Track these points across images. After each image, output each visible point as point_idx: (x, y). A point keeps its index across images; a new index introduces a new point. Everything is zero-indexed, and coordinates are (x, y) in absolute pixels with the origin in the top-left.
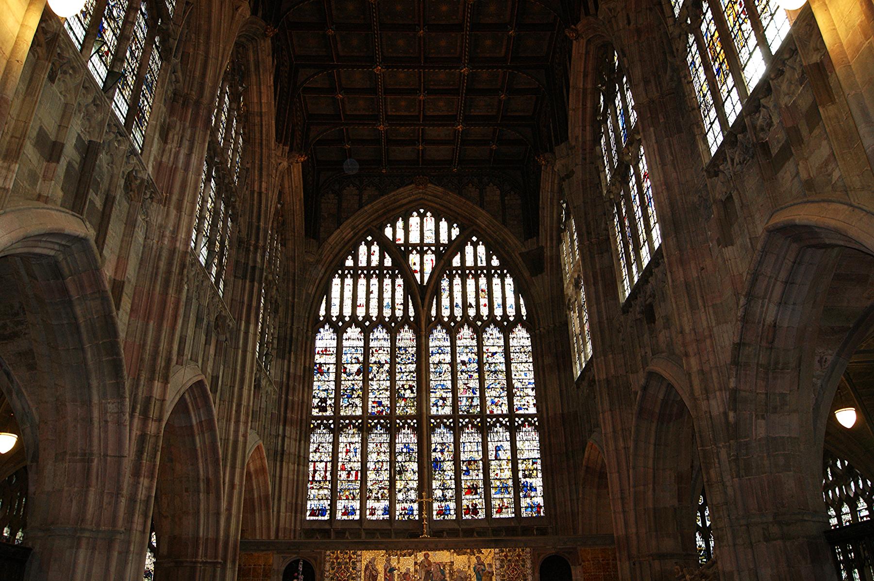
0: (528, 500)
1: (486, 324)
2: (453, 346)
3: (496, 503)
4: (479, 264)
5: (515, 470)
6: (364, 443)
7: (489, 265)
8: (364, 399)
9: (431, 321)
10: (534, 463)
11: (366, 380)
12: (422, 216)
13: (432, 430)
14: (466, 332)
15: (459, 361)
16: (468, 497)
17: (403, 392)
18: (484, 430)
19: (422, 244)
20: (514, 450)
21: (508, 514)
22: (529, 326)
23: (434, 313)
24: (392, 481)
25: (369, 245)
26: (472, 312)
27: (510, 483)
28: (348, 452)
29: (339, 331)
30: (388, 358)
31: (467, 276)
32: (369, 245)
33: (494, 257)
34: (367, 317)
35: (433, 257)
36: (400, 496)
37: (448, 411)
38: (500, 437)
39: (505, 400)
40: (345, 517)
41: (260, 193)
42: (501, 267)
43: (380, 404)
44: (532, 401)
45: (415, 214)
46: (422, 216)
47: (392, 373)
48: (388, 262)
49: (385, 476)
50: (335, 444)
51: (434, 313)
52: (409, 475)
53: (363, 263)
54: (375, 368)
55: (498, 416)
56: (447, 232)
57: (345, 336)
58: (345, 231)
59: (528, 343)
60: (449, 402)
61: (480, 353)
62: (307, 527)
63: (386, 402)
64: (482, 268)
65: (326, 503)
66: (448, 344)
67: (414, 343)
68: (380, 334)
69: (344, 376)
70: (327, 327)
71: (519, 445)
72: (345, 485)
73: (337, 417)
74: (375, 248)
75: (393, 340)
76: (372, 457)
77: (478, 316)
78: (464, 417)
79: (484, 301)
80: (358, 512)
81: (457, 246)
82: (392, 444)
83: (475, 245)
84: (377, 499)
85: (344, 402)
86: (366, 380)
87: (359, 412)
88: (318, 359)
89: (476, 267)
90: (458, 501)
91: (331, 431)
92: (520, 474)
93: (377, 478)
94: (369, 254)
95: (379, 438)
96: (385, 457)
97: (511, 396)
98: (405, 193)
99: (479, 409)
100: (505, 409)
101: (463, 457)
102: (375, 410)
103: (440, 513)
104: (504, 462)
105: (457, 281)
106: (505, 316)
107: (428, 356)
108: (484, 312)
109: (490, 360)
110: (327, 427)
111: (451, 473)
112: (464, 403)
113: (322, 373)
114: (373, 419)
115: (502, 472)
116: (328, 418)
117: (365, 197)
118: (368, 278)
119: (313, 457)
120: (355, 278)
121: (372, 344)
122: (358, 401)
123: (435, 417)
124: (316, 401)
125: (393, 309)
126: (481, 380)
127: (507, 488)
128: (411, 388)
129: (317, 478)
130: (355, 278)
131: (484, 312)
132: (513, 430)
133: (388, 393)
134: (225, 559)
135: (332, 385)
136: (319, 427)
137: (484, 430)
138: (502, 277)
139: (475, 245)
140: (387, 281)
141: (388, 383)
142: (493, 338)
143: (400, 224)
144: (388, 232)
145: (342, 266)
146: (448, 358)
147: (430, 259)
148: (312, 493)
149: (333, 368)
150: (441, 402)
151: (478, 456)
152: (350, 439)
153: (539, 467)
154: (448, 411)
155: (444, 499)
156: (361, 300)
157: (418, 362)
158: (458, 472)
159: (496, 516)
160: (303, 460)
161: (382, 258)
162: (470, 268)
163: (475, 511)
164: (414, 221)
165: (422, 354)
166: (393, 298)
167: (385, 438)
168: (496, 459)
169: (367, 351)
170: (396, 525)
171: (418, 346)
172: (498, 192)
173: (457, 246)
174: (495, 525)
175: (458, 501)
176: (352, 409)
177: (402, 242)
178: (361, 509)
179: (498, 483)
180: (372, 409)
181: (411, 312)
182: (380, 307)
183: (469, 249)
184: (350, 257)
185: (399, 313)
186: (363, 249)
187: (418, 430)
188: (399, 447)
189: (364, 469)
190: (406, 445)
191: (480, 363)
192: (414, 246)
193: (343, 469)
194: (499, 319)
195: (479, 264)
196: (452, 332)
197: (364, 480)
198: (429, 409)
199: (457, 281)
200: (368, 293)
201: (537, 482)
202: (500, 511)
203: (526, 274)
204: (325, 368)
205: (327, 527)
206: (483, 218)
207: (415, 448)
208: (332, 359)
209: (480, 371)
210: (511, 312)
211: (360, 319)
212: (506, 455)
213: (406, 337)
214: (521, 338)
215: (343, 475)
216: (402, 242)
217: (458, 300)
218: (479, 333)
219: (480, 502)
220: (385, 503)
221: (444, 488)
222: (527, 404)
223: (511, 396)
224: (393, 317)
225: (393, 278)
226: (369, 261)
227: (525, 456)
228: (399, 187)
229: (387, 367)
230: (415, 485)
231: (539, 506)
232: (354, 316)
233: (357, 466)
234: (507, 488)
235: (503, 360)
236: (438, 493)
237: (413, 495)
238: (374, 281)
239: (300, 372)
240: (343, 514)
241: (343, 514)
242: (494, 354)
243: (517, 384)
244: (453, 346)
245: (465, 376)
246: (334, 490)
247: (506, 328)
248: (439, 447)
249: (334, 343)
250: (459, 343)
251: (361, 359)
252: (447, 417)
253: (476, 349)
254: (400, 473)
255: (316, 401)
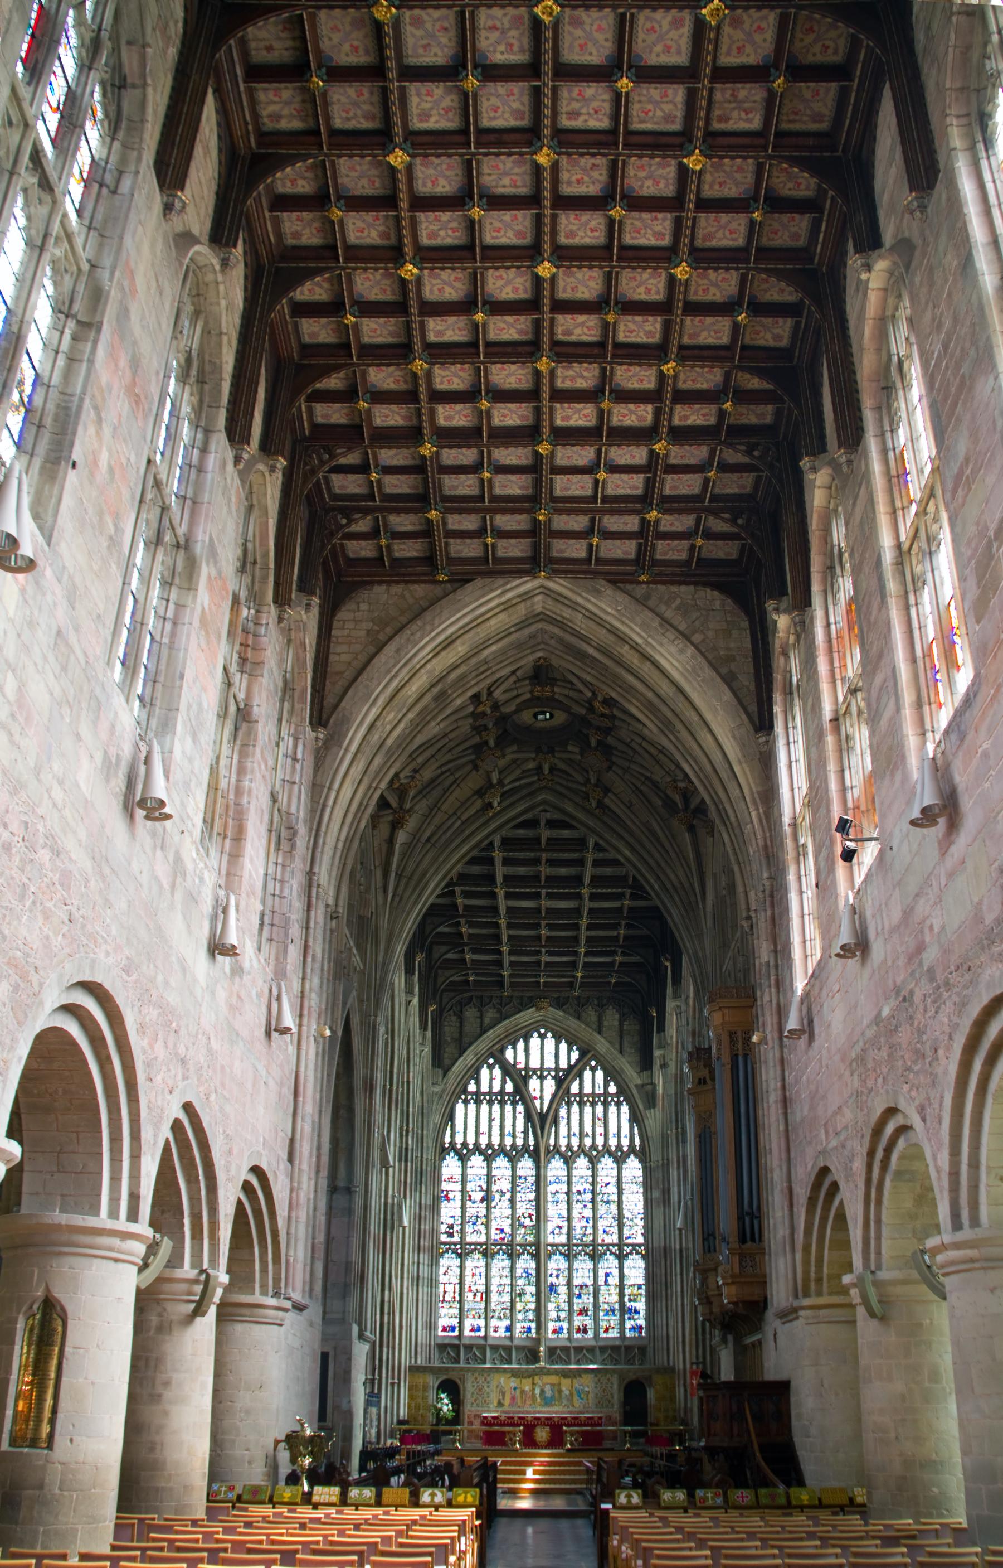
0: (632, 1322)
1: (601, 1154)
2: (569, 1176)
3: (603, 1324)
4: (597, 1092)
5: (621, 1295)
6: (487, 1266)
7: (606, 1094)
8: (487, 1225)
9: (548, 1152)
10: (640, 1288)
11: (488, 1208)
12: (543, 1037)
13: (549, 1256)
14: (582, 1162)
15: (574, 1190)
16: (581, 1318)
17: (522, 1220)
18: (595, 1257)
19: (542, 1069)
20: (622, 1276)
21: (614, 1334)
22: (643, 1156)
23: (552, 1142)
24: (513, 1302)
25: (491, 1067)
26: (588, 1142)
27: (617, 1306)
28: (473, 1275)
29: (463, 1159)
30: (509, 1186)
31: (585, 1103)
32: (491, 1067)
33: (612, 1084)
34: (490, 1145)
35: (553, 1082)
36: (520, 1316)
37: (563, 1239)
38: (609, 1264)
39: (615, 1230)
40: (473, 1334)
41: (408, 1082)
42: (618, 1094)
43: (502, 1231)
44: (640, 1230)
45: (536, 1035)
46: (543, 1037)
47: (512, 1201)
48: (509, 1087)
49: (506, 1298)
50: (462, 1267)
51: (552, 1142)
52: (528, 1297)
53: (485, 1088)
54: (497, 1196)
55: (608, 1245)
56: (567, 1056)
57: (469, 1164)
58: (468, 1058)
59: (640, 1173)
60: (565, 1230)
61: (593, 1184)
62: (439, 1341)
63: (508, 1230)
64: (599, 1096)
65: (455, 1322)
66: (565, 1173)
67: (534, 1173)
68: (501, 1163)
69: (469, 1204)
70: (452, 1154)
71: (626, 1271)
72: (472, 1305)
73: (462, 1243)
74: (497, 1072)
75: (514, 1169)
76: (495, 1282)
77: (594, 1146)
78: (577, 1245)
79: (600, 1130)
80: (483, 1330)
81: (575, 1071)
82: (512, 1269)
83: (593, 1070)
84: (500, 1318)
85: (469, 1229)
86: (488, 1208)
87: (483, 1239)
88: (444, 1186)
89: (593, 1094)
90: (570, 1320)
91: (459, 1255)
92: (626, 1299)
93: (499, 1300)
94: (491, 1079)
95: (500, 1263)
96: (508, 1281)
97: (621, 1226)
98: (527, 1016)
99: (591, 1238)
100: (615, 1239)
101: (576, 1282)
102: (497, 1237)
103: (555, 1331)
104: (612, 1288)
105: (575, 1108)
106: (619, 1147)
107: (546, 1186)
108: (600, 1141)
109: (604, 1190)
110: (455, 1252)
111: (565, 1297)
112: (578, 1232)
113: (448, 1199)
114: (496, 1245)
115: (610, 1296)
116: (455, 1244)
117: (487, 1020)
118: (490, 1103)
119: (442, 1279)
120: (478, 1102)
121: (494, 1172)
122: (482, 1228)
123: (552, 1245)
124: (443, 1228)
125: (514, 1136)
126: (594, 1209)
127: (613, 1311)
128: (530, 1215)
129: (448, 1298)
130: (478, 1102)
131: (600, 1141)
132: (621, 1257)
133: (509, 1221)
134: (399, 1379)
135: (458, 1212)
136: (447, 1251)
137: (595, 1257)
138: (618, 1104)
139: (593, 1070)
140: (508, 1108)
141: (509, 1212)
142: (607, 1166)
143: (521, 1045)
144: (509, 1054)
145: (465, 1091)
146: (564, 1188)
147: (550, 1085)
148: (443, 1312)
149: (459, 1196)
150: (557, 1231)
151: (590, 1282)
152: (475, 1263)
153: (643, 1291)
154: (563, 1239)
155: (559, 1319)
156: (484, 1127)
157: (538, 1191)
158: (570, 1295)
159: (603, 1335)
160: (433, 1282)
161: (504, 1082)
162: (587, 1095)
163: (585, 1331)
164: (535, 1041)
165: (539, 1183)
166: (514, 1125)
167: (507, 1263)
168: (606, 1283)
169: (489, 1176)
170: (516, 1342)
171: (538, 1176)
172: (617, 1016)
173: (575, 1071)
174: (601, 1343)
175: (570, 1320)
176: (475, 1236)
177: (522, 1066)
178: (486, 1326)
179: (606, 1306)
180: (495, 1236)
181: (531, 1141)
182: (502, 1135)
183: (587, 1074)
184: (473, 1082)
185: (520, 1142)
186: (485, 1072)
187: (536, 1257)
188: (519, 1272)
189: (488, 1291)
190: (526, 1271)
191: (593, 1192)
192: (535, 1071)
193: (470, 1291)
194: (613, 1149)
195: (597, 1092)
196: (568, 1161)
197: (487, 1302)
198: (545, 1237)
199: (575, 1108)
200: (491, 1120)
201: (641, 1305)
202: (606, 1331)
203: (641, 1106)
204: (451, 1195)
205: (457, 1342)
206: (602, 1045)
207: (534, 1273)
208: (458, 1187)
209: (593, 1201)
210: (625, 1142)
211: (483, 1147)
212: (614, 1280)
213: (526, 1166)
214: (633, 1168)
215: (469, 1296)
216: (522, 1066)
217: (575, 1129)
218: (593, 1162)
219: (589, 1322)
220: (508, 1322)
221: (559, 1309)
222: (636, 1233)
223: (621, 1226)
224: (514, 1146)
225: (514, 1103)
226: (491, 1087)
227: (631, 1282)
228: (520, 1011)
229: (508, 1195)
230: (533, 1306)
231: (641, 1327)
232: (477, 1145)
233: (482, 1288)
234: (613, 1311)
235: (615, 1191)
236: (553, 1315)
237: (531, 1315)
238: (496, 1107)
239: (430, 1202)
240: (472, 1330)
241: (472, 1330)
242: (607, 1184)
243: (626, 1214)
244: (569, 1176)
245: (580, 1205)
246: (461, 1309)
247: (619, 1158)
248: (555, 1273)
249: (459, 1171)
250: (575, 1172)
251: (485, 1187)
252: (563, 1245)
253: (590, 1180)
254: (520, 1295)
255: (443, 1228)
